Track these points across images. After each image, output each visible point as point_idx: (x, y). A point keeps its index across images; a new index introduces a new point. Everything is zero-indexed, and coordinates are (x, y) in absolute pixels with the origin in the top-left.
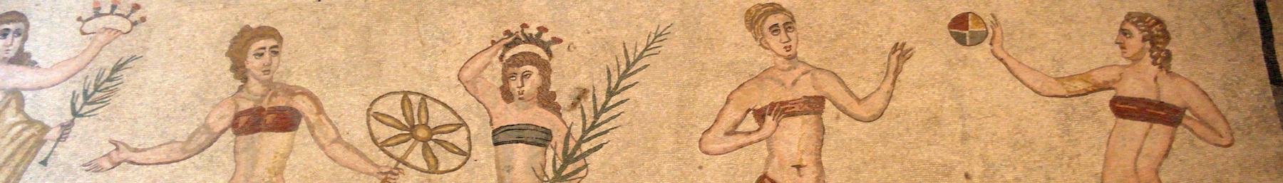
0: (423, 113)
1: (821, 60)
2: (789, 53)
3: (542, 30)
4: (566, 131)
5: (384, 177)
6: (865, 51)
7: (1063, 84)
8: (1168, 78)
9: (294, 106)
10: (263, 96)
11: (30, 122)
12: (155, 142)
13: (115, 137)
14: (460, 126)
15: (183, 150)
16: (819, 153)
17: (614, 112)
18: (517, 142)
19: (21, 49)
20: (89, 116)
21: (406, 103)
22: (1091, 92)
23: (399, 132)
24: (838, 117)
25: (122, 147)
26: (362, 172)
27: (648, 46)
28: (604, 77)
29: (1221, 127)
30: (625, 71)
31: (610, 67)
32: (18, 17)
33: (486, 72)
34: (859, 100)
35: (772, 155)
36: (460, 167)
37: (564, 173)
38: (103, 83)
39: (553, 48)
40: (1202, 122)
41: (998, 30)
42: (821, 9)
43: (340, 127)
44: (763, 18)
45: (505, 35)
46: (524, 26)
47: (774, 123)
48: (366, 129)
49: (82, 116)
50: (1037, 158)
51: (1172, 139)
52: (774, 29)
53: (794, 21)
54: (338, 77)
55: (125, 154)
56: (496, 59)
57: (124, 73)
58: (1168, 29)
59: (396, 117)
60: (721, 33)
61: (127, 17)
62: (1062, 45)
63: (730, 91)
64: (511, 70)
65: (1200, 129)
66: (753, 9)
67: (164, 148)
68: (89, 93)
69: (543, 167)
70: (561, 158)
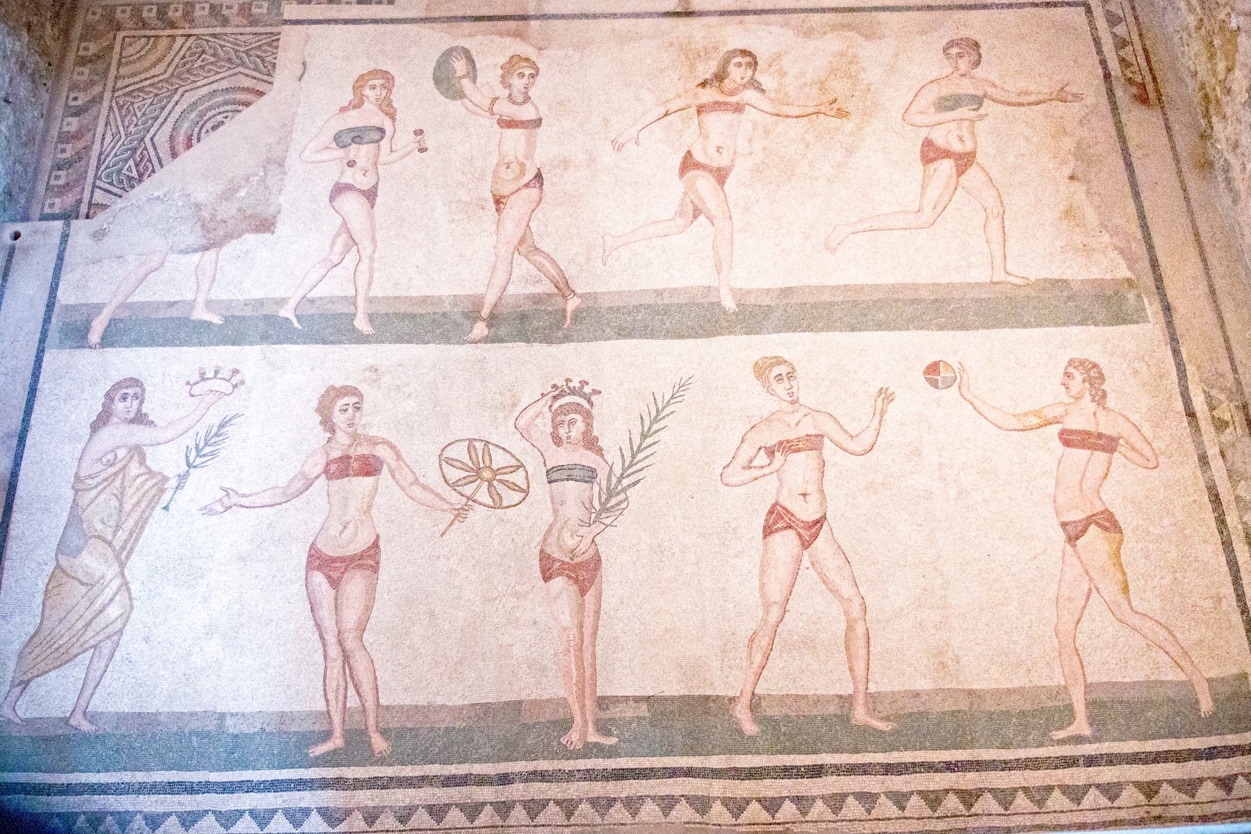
0: (487, 458)
2: (792, 399)
5: (457, 512)
7: (1019, 420)
8: (1104, 412)
9: (376, 454)
10: (350, 446)
11: (151, 473)
13: (226, 485)
14: (518, 467)
15: (284, 494)
17: (649, 451)
19: (139, 410)
22: (1042, 426)
23: (468, 474)
25: (231, 492)
32: (135, 382)
33: (539, 420)
34: (851, 437)
37: (608, 506)
39: (593, 398)
40: (1133, 449)
41: (965, 376)
45: (552, 388)
46: (568, 380)
48: (439, 473)
49: (195, 467)
51: (1110, 463)
52: (780, 377)
55: (235, 499)
56: (546, 409)
57: (228, 429)
58: (1103, 372)
61: (228, 381)
63: (744, 432)
64: (559, 419)
65: (1130, 454)
66: (760, 361)
67: (267, 493)
68: (200, 447)
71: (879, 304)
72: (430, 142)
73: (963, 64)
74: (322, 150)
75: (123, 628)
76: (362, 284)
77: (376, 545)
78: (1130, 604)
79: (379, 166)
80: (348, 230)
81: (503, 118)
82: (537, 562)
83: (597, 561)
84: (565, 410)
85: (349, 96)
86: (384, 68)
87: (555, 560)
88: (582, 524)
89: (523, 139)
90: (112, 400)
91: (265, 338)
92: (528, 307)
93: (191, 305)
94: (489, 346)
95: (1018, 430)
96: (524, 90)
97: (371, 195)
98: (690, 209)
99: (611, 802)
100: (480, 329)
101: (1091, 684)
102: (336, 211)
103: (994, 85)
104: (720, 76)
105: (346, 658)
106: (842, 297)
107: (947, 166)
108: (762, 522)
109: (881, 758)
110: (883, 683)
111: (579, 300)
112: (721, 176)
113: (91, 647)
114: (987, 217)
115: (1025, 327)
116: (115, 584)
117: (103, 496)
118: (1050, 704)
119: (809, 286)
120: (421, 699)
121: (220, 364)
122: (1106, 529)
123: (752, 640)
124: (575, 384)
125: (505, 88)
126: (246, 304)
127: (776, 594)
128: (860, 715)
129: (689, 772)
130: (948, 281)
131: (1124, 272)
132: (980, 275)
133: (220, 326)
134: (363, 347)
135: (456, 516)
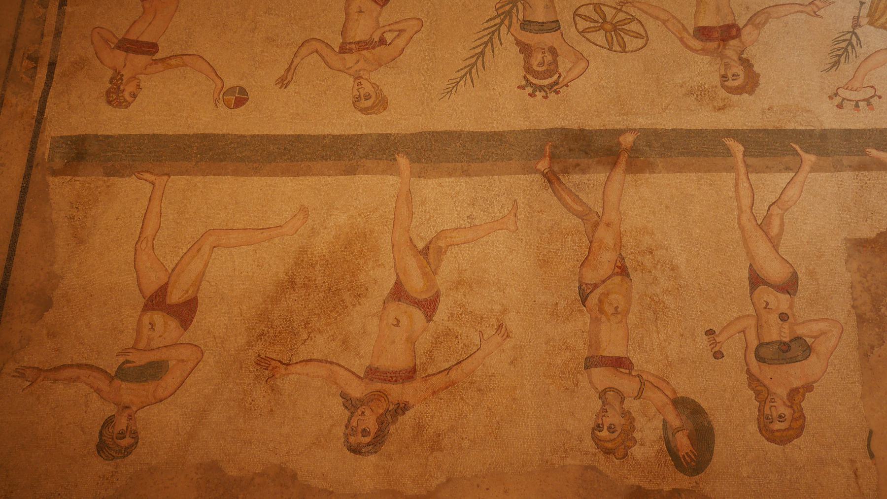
0: (610, 39)
2: (359, 81)
7: (183, 62)
9: (700, 43)
10: (725, 48)
14: (583, 31)
16: (347, 20)
17: (479, 43)
18: (543, 23)
20: (844, 32)
21: (623, 45)
22: (168, 58)
23: (624, 27)
25: (813, 14)
26: (644, 3)
27: (457, 85)
28: (487, 64)
30: (472, 68)
31: (483, 70)
33: (569, 66)
34: (317, 51)
35: (377, 18)
36: (579, 7)
37: (511, 5)
38: (843, 53)
39: (524, 83)
40: (106, 41)
41: (216, 96)
42: (334, 111)
44: (375, 104)
46: (546, 97)
48: (646, 28)
49: (849, 32)
51: (128, 31)
53: (353, 103)
55: (809, 9)
56: (564, 75)
59: (628, 36)
61: (844, 99)
63: (401, 56)
64: (552, 67)
66: (382, 111)
67: (783, 14)
68: (850, 46)
69: (524, 8)
70: (513, 14)
72: (702, 341)
73: (122, 423)
76: (744, 185)
79: (751, 311)
80: (770, 240)
81: (627, 371)
85: (809, 403)
86: (774, 446)
91: (824, 135)
94: (617, 127)
95: (187, 55)
96: (606, 407)
97: (756, 280)
100: (628, 140)
102: (788, 263)
103: (98, 391)
107: (175, 296)
111: (539, 166)
112: (399, 293)
114: (154, 239)
119: (329, 176)
131: (53, 181)
132: (179, 182)
134: (730, 126)
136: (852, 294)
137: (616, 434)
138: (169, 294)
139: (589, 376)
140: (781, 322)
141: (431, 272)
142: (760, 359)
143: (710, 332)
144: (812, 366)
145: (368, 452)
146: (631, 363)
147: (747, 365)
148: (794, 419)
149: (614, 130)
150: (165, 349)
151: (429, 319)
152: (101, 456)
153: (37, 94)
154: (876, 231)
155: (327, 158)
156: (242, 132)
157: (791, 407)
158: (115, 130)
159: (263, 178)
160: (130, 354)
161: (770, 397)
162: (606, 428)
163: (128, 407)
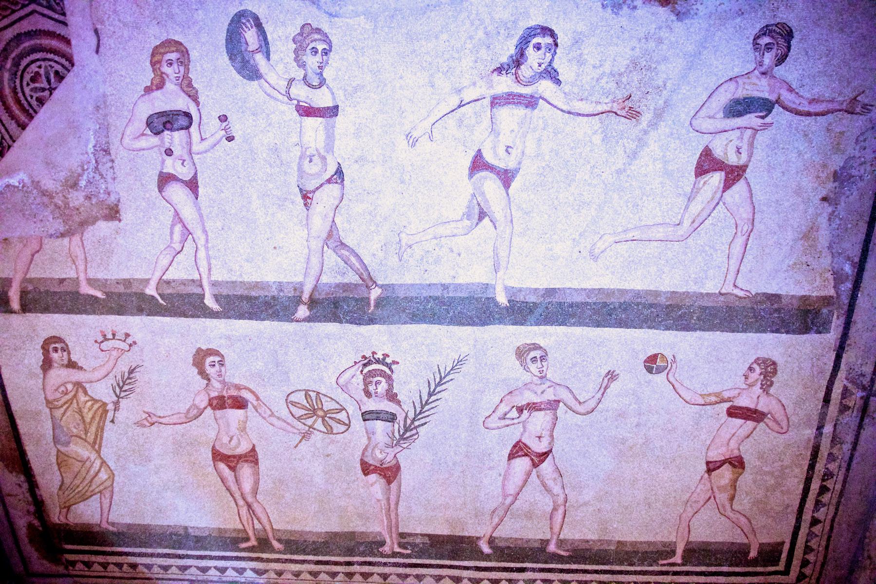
0: (319, 402)
1: (560, 379)
3: (386, 356)
4: (405, 415)
6: (589, 375)
11: (96, 401)
12: (169, 413)
13: (146, 410)
15: (186, 417)
17: (433, 405)
24: (566, 412)
27: (453, 367)
29: (784, 424)
30: (439, 382)
33: (354, 380)
34: (580, 403)
35: (525, 431)
39: (393, 367)
41: (674, 366)
43: (271, 408)
46: (374, 353)
47: (528, 414)
49: (122, 398)
50: (676, 436)
51: (755, 429)
54: (264, 380)
55: (155, 419)
56: (359, 372)
60: (500, 361)
61: (124, 341)
62: (711, 375)
65: (771, 423)
67: (175, 416)
69: (393, 434)
71: (625, 307)
72: (237, 130)
73: (768, 59)
74: (139, 136)
75: (113, 483)
76: (204, 270)
77: (253, 450)
78: (731, 506)
79: (196, 157)
80: (181, 221)
81: (301, 104)
82: (358, 466)
83: (397, 468)
84: (373, 374)
85: (147, 76)
86: (176, 38)
87: (371, 465)
88: (388, 446)
89: (321, 128)
90: (48, 351)
91: (140, 311)
92: (341, 294)
93: (76, 281)
94: (312, 324)
96: (319, 71)
97: (193, 185)
98: (477, 211)
99: (407, 576)
101: (691, 542)
102: (166, 200)
103: (791, 90)
104: (518, 60)
105: (249, 506)
106: (595, 299)
107: (716, 179)
108: (508, 451)
109: (560, 566)
110: (568, 534)
112: (506, 177)
113: (98, 492)
114: (736, 233)
115: (733, 331)
116: (98, 463)
117: (68, 413)
118: (663, 549)
120: (297, 527)
121: (115, 329)
122: (734, 466)
123: (494, 512)
124: (379, 356)
125: (299, 66)
126: (118, 283)
127: (512, 489)
128: (552, 548)
129: (451, 567)
130: (684, 290)
132: (711, 286)
133: (104, 300)
134: (215, 322)
135: (303, 437)
136: (114, 173)
137: (310, 47)
138: (722, 182)
139: (334, 99)
140: (171, 148)
141: (477, 196)
142: (188, 115)
143: (230, 139)
144: (145, 110)
145: (536, 29)
146: (298, 111)
147: (199, 110)
148: (159, 62)
149: (314, 321)
150: (726, 129)
151: (479, 155)
152: (789, 27)
153: (842, 374)
154: (96, 226)
155: (571, 305)
156: (651, 331)
157: (162, 73)
158: (769, 337)
159: (632, 288)
160: (760, 124)
161: (180, 81)
162: (320, 52)
163: (763, 74)
